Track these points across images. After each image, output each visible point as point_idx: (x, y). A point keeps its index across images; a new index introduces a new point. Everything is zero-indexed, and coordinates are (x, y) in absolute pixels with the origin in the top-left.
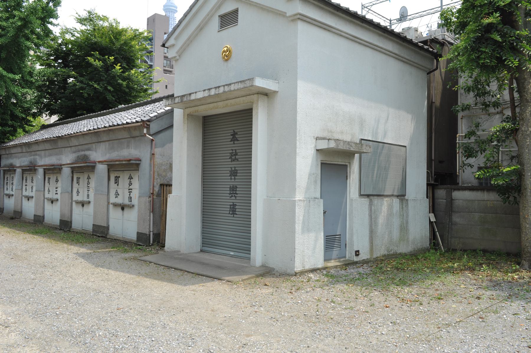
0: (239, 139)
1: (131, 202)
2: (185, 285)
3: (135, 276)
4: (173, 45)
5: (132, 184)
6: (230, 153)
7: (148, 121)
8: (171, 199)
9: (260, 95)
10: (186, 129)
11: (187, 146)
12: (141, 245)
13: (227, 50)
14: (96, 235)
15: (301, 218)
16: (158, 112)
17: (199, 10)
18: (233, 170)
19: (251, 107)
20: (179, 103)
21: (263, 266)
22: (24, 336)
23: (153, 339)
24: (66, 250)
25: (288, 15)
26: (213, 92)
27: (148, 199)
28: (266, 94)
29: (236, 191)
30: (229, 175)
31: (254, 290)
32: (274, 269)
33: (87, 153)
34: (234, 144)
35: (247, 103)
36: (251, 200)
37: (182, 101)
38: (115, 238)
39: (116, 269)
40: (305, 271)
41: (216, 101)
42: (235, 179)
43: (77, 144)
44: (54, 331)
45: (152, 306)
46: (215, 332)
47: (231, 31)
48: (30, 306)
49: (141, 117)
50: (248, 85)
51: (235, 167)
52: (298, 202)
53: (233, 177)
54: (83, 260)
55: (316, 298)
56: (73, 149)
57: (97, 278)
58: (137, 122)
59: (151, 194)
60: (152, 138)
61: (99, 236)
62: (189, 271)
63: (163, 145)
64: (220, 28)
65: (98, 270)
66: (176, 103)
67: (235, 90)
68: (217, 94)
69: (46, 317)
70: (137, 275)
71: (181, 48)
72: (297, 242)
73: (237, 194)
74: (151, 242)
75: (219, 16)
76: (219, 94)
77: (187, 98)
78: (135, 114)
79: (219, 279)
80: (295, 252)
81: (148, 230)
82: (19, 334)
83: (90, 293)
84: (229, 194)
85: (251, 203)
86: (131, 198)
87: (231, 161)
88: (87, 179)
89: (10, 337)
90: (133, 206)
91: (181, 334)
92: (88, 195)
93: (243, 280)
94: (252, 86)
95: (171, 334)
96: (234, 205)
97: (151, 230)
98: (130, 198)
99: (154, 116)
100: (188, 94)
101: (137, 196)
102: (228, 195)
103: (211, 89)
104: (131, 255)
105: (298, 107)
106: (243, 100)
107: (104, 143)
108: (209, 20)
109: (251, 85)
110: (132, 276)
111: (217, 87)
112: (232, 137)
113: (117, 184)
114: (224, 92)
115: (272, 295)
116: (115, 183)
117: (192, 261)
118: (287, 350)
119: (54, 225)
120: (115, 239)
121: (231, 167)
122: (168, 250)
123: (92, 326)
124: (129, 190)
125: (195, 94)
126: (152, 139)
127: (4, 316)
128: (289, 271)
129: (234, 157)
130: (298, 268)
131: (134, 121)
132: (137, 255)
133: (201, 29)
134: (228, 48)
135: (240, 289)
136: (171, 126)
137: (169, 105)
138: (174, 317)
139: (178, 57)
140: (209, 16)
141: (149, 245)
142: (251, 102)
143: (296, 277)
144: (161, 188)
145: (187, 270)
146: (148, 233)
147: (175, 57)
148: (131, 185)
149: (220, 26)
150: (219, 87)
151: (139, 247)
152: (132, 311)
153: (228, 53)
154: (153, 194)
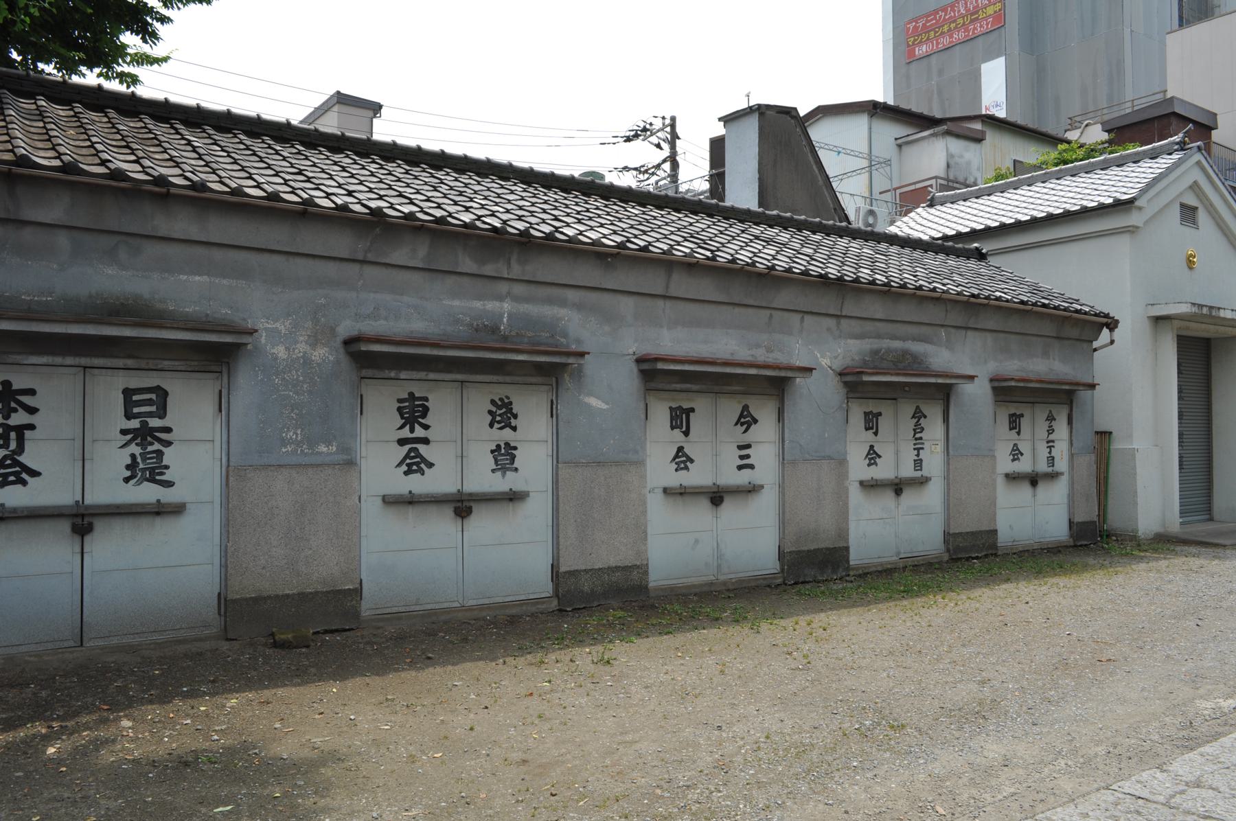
0: (1184, 372)
1: (1053, 466)
5: (1053, 430)
33: (917, 347)
38: (1021, 549)
43: (878, 316)
56: (855, 326)
86: (1053, 458)
88: (913, 417)
92: (918, 464)
98: (1051, 460)
107: (977, 334)
113: (1017, 430)
116: (1011, 429)
119: (741, 581)
124: (1048, 442)
148: (1052, 433)
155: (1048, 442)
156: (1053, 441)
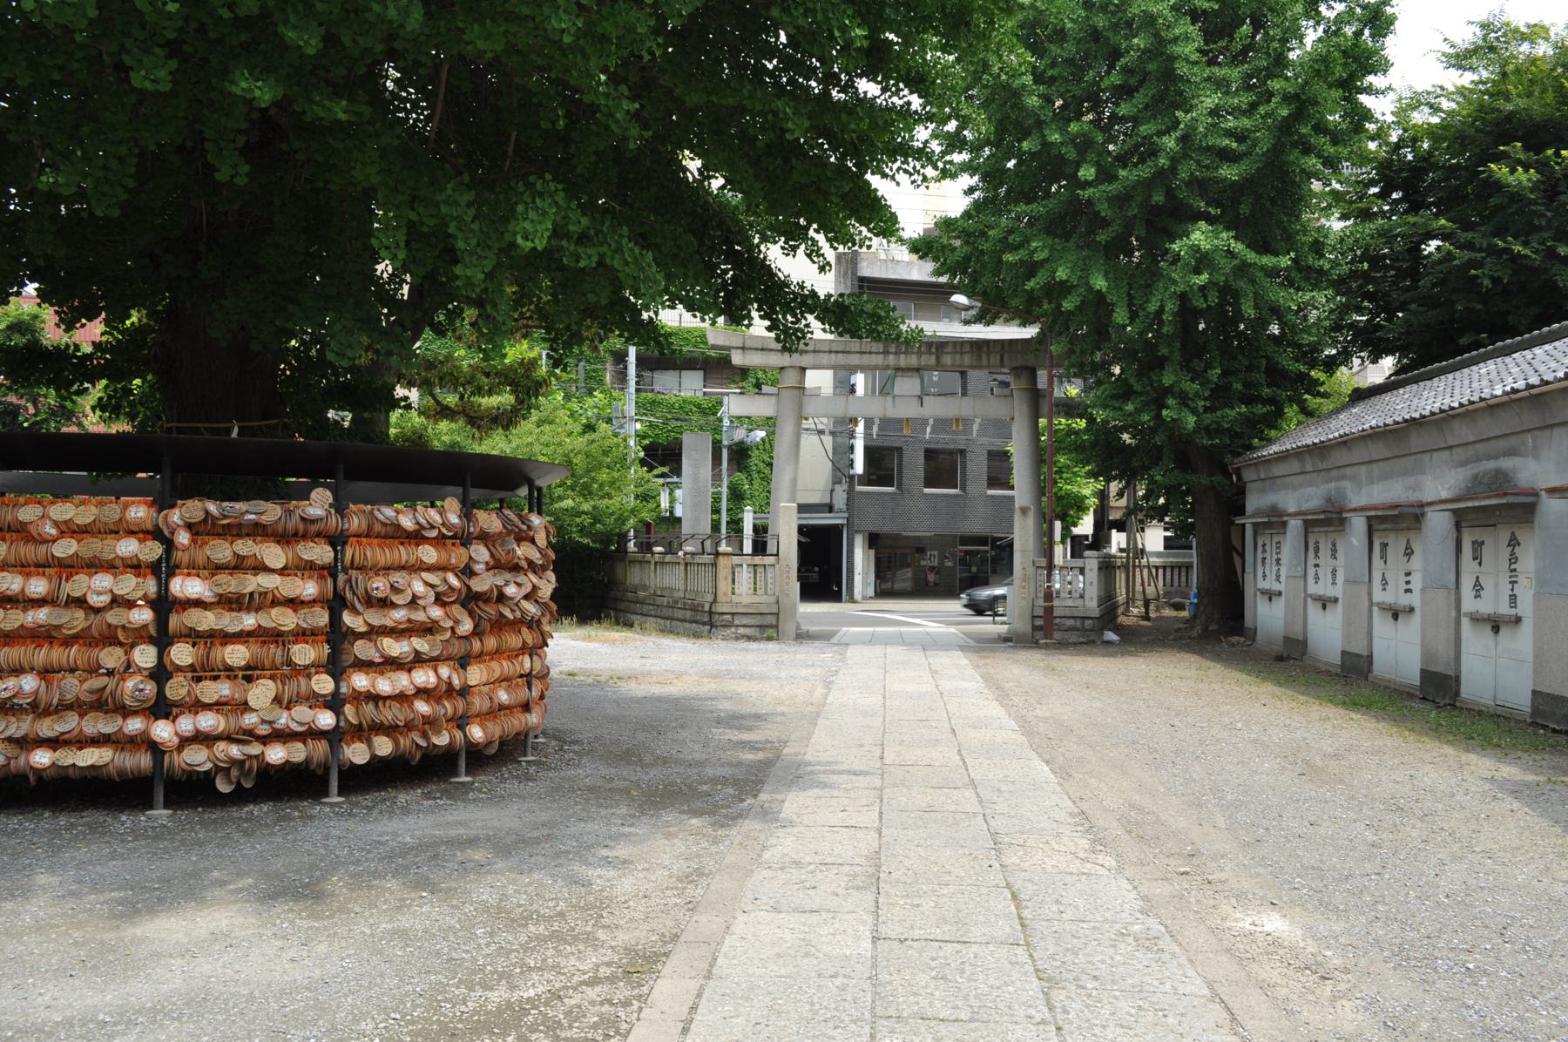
14: (1544, 727)
22: (1381, 1017)
24: (1455, 766)
33: (1506, 464)
43: (1471, 439)
44: (1472, 1026)
48: (1382, 928)
54: (1516, 805)
56: (1459, 454)
61: (1554, 731)
82: (1366, 1009)
88: (1509, 545)
89: (1339, 1010)
92: (1513, 599)
119: (1401, 685)
127: (1310, 942)
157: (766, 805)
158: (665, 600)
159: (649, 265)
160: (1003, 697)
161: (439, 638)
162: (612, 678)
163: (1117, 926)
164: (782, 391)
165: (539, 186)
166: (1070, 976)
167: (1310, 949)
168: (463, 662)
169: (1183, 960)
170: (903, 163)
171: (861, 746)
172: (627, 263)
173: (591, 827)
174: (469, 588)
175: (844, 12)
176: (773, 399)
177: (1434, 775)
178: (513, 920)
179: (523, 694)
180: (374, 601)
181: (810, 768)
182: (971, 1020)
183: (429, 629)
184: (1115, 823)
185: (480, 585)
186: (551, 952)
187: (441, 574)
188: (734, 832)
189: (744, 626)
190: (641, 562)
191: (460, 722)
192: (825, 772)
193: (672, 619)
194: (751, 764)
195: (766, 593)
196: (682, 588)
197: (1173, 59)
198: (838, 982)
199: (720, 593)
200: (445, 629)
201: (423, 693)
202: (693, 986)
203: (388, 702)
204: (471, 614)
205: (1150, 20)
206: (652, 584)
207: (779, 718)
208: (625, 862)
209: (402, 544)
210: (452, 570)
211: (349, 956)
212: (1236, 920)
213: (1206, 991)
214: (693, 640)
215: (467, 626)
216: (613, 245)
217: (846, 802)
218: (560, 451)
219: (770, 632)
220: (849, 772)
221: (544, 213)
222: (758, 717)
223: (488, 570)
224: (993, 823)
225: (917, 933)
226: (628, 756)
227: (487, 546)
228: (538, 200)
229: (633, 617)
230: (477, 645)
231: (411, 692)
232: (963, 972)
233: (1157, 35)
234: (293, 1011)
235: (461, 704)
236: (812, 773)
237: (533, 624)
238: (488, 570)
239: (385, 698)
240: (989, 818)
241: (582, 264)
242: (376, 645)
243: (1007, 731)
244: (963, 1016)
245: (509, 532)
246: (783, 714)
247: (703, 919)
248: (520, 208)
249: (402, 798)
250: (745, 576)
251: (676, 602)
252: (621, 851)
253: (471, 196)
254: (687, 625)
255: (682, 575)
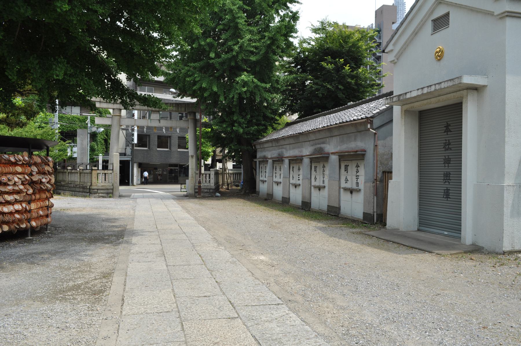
0: (452, 130)
1: (358, 186)
2: (399, 254)
3: (360, 245)
4: (392, 51)
5: (358, 171)
6: (444, 143)
7: (372, 117)
8: (392, 184)
9: (469, 91)
10: (403, 123)
11: (405, 138)
12: (367, 224)
13: (440, 51)
14: (330, 214)
15: (510, 202)
16: (380, 109)
17: (414, 17)
18: (447, 158)
19: (459, 102)
20: (396, 101)
21: (473, 245)
23: (369, 283)
24: (307, 224)
25: (495, 14)
26: (425, 91)
27: (372, 184)
28: (476, 89)
29: (449, 177)
30: (443, 162)
31: (459, 262)
32: (483, 248)
33: (322, 146)
34: (447, 134)
35: (458, 97)
36: (461, 185)
37: (399, 100)
38: (346, 217)
39: (345, 239)
40: (514, 251)
41: (429, 97)
42: (448, 166)
43: (314, 139)
45: (370, 265)
46: (417, 285)
47: (443, 33)
49: (366, 113)
50: (457, 83)
51: (448, 156)
52: (506, 187)
53: (446, 165)
54: (320, 232)
55: (518, 272)
57: (331, 244)
58: (362, 119)
59: (375, 180)
60: (375, 132)
61: (332, 215)
62: (405, 244)
63: (385, 138)
64: (433, 31)
65: (331, 239)
66: (394, 102)
67: (445, 88)
68: (429, 92)
69: (296, 263)
70: (361, 244)
71: (399, 52)
72: (505, 224)
73: (450, 180)
74: (375, 221)
75: (432, 21)
76: (430, 92)
77: (403, 97)
78: (361, 111)
79: (430, 252)
80: (503, 232)
81: (372, 211)
83: (326, 253)
84: (443, 179)
85: (461, 188)
86: (358, 183)
87: (445, 151)
90: (360, 190)
91: (390, 283)
92: (324, 181)
93: (451, 254)
94: (460, 83)
95: (382, 282)
96: (448, 190)
97: (375, 211)
98: (357, 184)
99: (377, 113)
100: (404, 93)
101: (363, 181)
102: (442, 181)
103: (424, 88)
104: (358, 230)
105: (506, 99)
106: (454, 96)
107: (335, 137)
108: (423, 24)
109: (459, 82)
110: (358, 245)
111: (429, 86)
112: (445, 128)
114: (436, 90)
115: (475, 267)
117: (409, 238)
118: (473, 301)
120: (345, 218)
121: (445, 156)
122: (389, 228)
123: (327, 271)
124: (356, 176)
125: (410, 93)
126: (375, 133)
128: (497, 250)
129: (447, 146)
130: (507, 247)
131: (360, 118)
132: (362, 231)
133: (416, 34)
134: (440, 49)
135: (447, 261)
136: (391, 121)
137: (388, 103)
138: (386, 273)
139: (396, 61)
140: (423, 22)
141: (373, 223)
142: (461, 97)
143: (504, 256)
144: (383, 175)
145: (403, 243)
146: (372, 213)
147: (394, 61)
149: (433, 29)
150: (431, 86)
151: (364, 225)
152: (355, 266)
153: (440, 53)
154: (376, 180)
155: (356, 176)
156: (358, 176)
157: (127, 240)
158: (72, 185)
159: (92, 85)
160: (188, 212)
161: (22, 195)
162: (61, 210)
163: (226, 260)
164: (114, 117)
165: (59, 60)
166: (216, 270)
167: (270, 262)
168: (29, 202)
169: (241, 265)
170: (165, 59)
171: (149, 225)
172: (85, 84)
173: (76, 248)
174: (32, 179)
175: (153, 19)
176: (111, 119)
177: (302, 226)
178: (66, 269)
179: (46, 212)
180: (2, 184)
181: (136, 231)
182: (194, 278)
183: (19, 192)
184: (223, 240)
185: (36, 178)
186: (81, 275)
187: (23, 175)
188: (120, 247)
189: (101, 193)
190: (62, 172)
191: (28, 221)
192: (141, 232)
193: (75, 191)
194: (118, 231)
195: (109, 182)
196: (79, 181)
197: (237, 23)
198: (160, 274)
199: (93, 182)
200: (24, 192)
201: (17, 212)
202: (123, 278)
203: (6, 215)
204: (32, 188)
205: (231, 11)
206: (67, 180)
207: (122, 219)
208: (91, 255)
209: (10, 166)
210: (26, 174)
211: (23, 279)
212: (254, 258)
213: (247, 270)
214: (84, 198)
215: (31, 191)
216: (81, 78)
217: (150, 239)
218: (32, 134)
219: (110, 195)
220: (148, 232)
221: (62, 68)
222: (115, 219)
223: (37, 174)
224: (191, 241)
225: (177, 264)
226: (78, 230)
227: (36, 167)
228: (59, 64)
229: (60, 191)
230: (34, 197)
231: (14, 211)
232: (190, 270)
233: (233, 15)
234: (16, 290)
235: (29, 215)
236: (137, 232)
237: (48, 190)
238: (37, 174)
239: (5, 213)
240: (190, 240)
241: (71, 83)
242: (3, 197)
243: (192, 220)
244: (192, 278)
245: (43, 162)
246: (123, 218)
247: (120, 265)
248: (54, 67)
249: (12, 244)
250: (102, 177)
251: (77, 186)
252: (89, 253)
253: (37, 62)
254: (81, 193)
255: (79, 176)
